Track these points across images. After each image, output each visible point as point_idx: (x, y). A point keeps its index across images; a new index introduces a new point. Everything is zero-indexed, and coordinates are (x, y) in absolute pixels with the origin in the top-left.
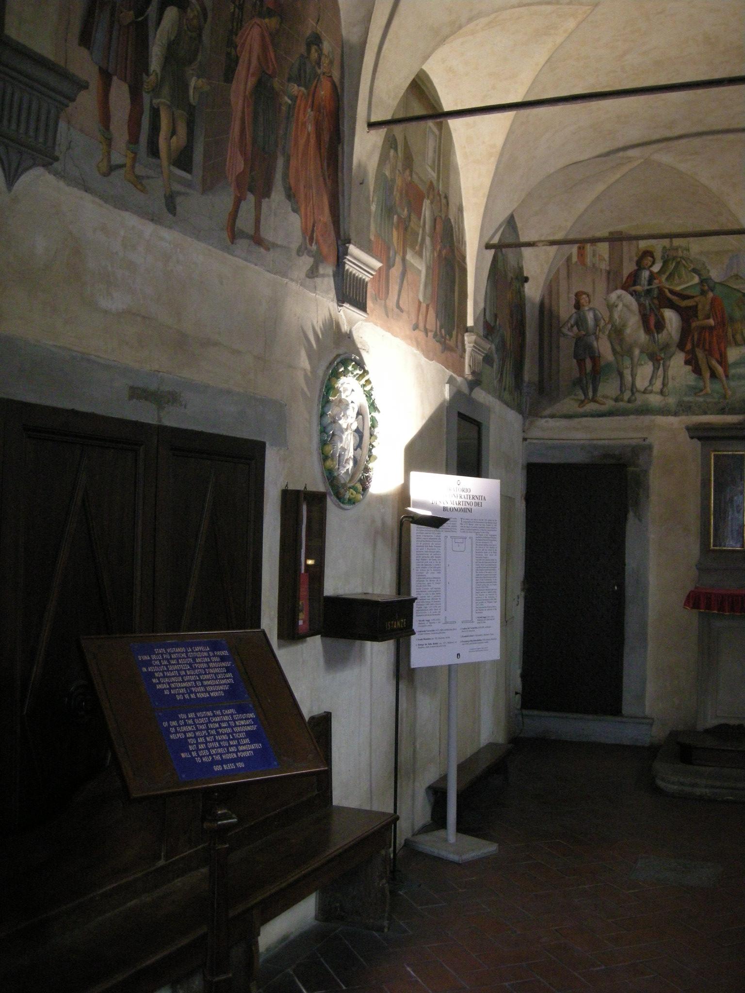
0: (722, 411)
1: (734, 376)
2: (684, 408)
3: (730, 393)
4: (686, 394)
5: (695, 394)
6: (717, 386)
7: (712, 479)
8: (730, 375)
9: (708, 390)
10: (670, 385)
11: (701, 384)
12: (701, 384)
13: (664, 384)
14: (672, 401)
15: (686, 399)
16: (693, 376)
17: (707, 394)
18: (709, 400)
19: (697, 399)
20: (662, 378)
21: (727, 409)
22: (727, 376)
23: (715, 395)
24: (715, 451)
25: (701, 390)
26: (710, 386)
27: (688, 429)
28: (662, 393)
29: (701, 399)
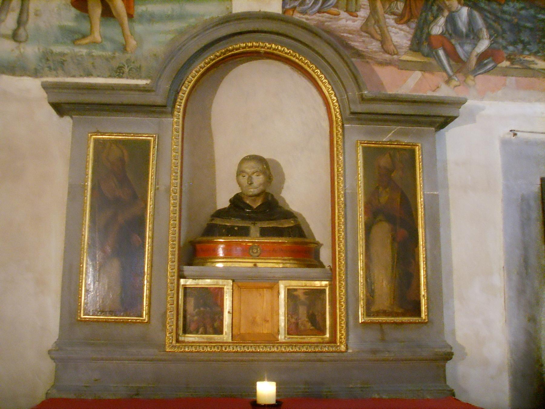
0: (119, 72)
1: (141, 16)
2: (51, 62)
3: (132, 42)
4: (57, 42)
5: (74, 42)
6: (113, 32)
7: (89, 184)
8: (135, 16)
9: (97, 36)
10: (31, 25)
11: (85, 26)
12: (85, 26)
13: (20, 22)
14: (31, 51)
15: (57, 49)
16: (74, 11)
17: (95, 43)
18: (96, 52)
19: (77, 49)
20: (17, 11)
21: (126, 70)
22: (130, 16)
23: (108, 45)
24: (97, 133)
25: (84, 36)
26: (99, 29)
27: (46, 87)
28: (15, 36)
29: (84, 51)
